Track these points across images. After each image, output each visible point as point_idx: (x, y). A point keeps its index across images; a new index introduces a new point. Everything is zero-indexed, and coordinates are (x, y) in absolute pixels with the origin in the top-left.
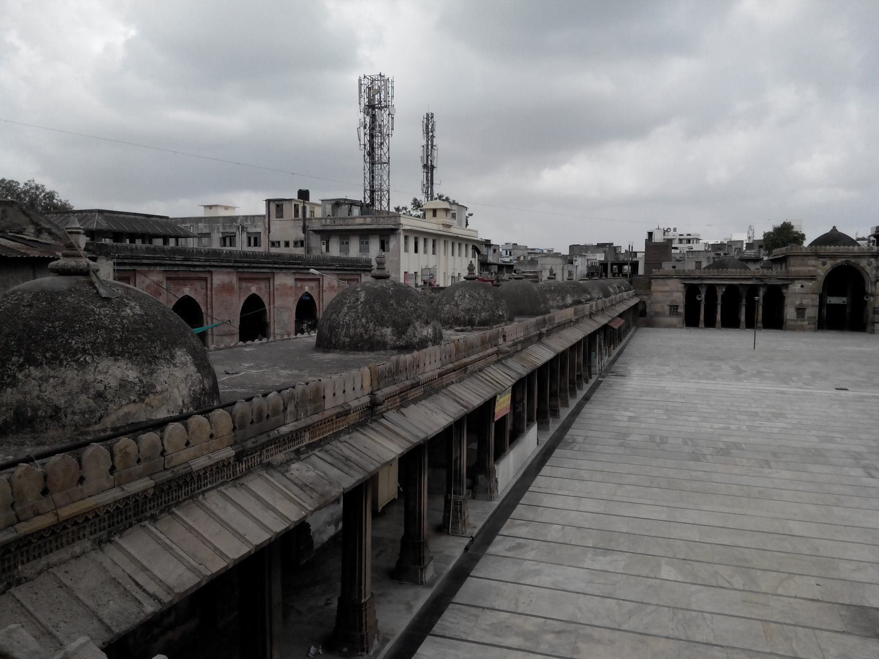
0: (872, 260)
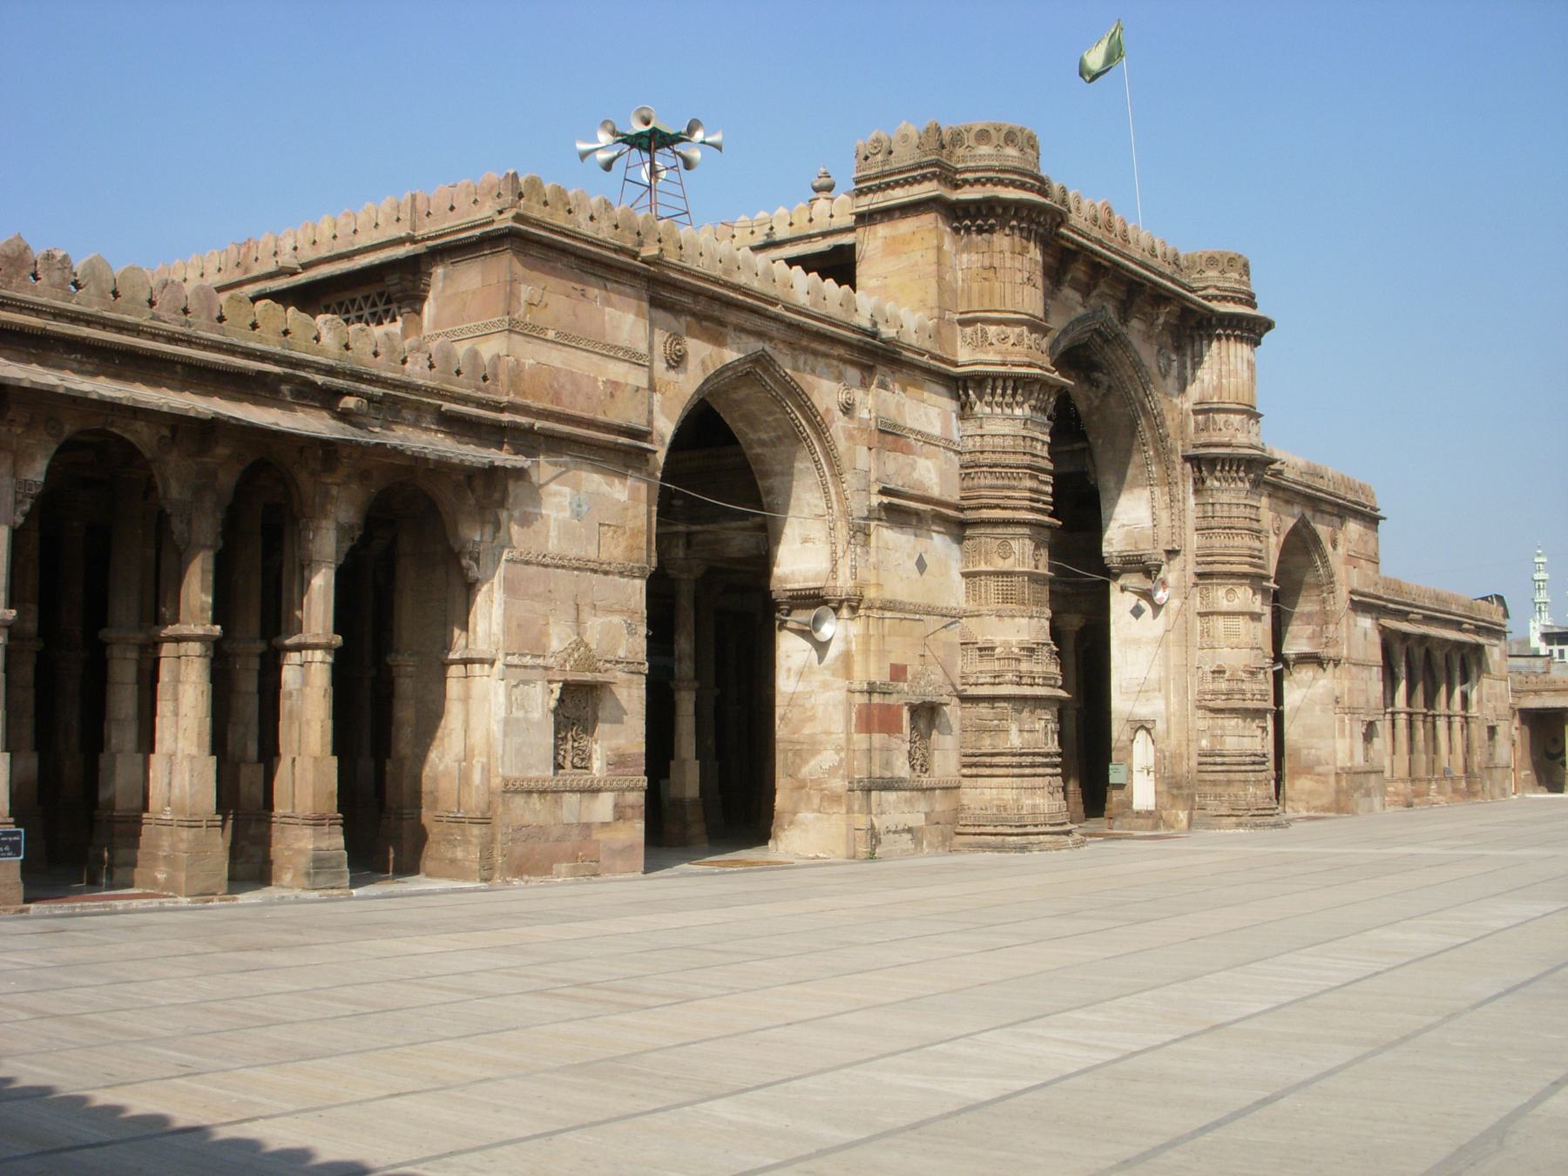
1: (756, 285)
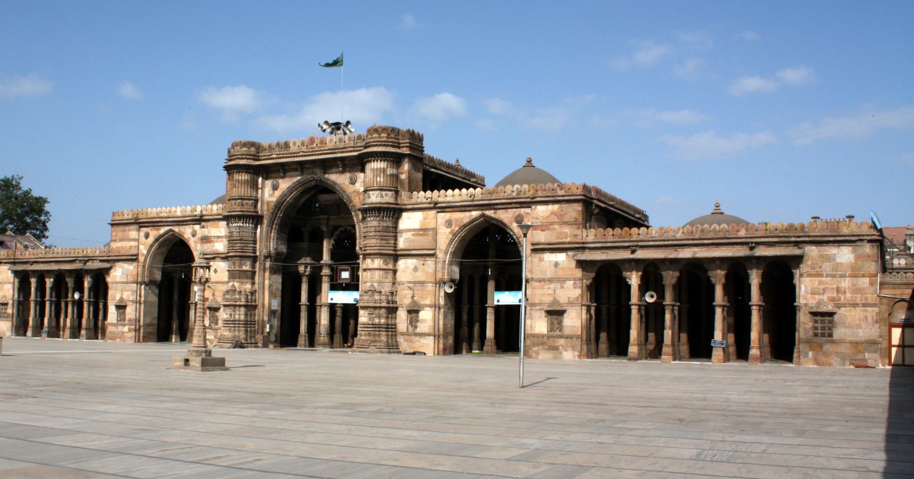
0: (197, 227)
1: (166, 215)
